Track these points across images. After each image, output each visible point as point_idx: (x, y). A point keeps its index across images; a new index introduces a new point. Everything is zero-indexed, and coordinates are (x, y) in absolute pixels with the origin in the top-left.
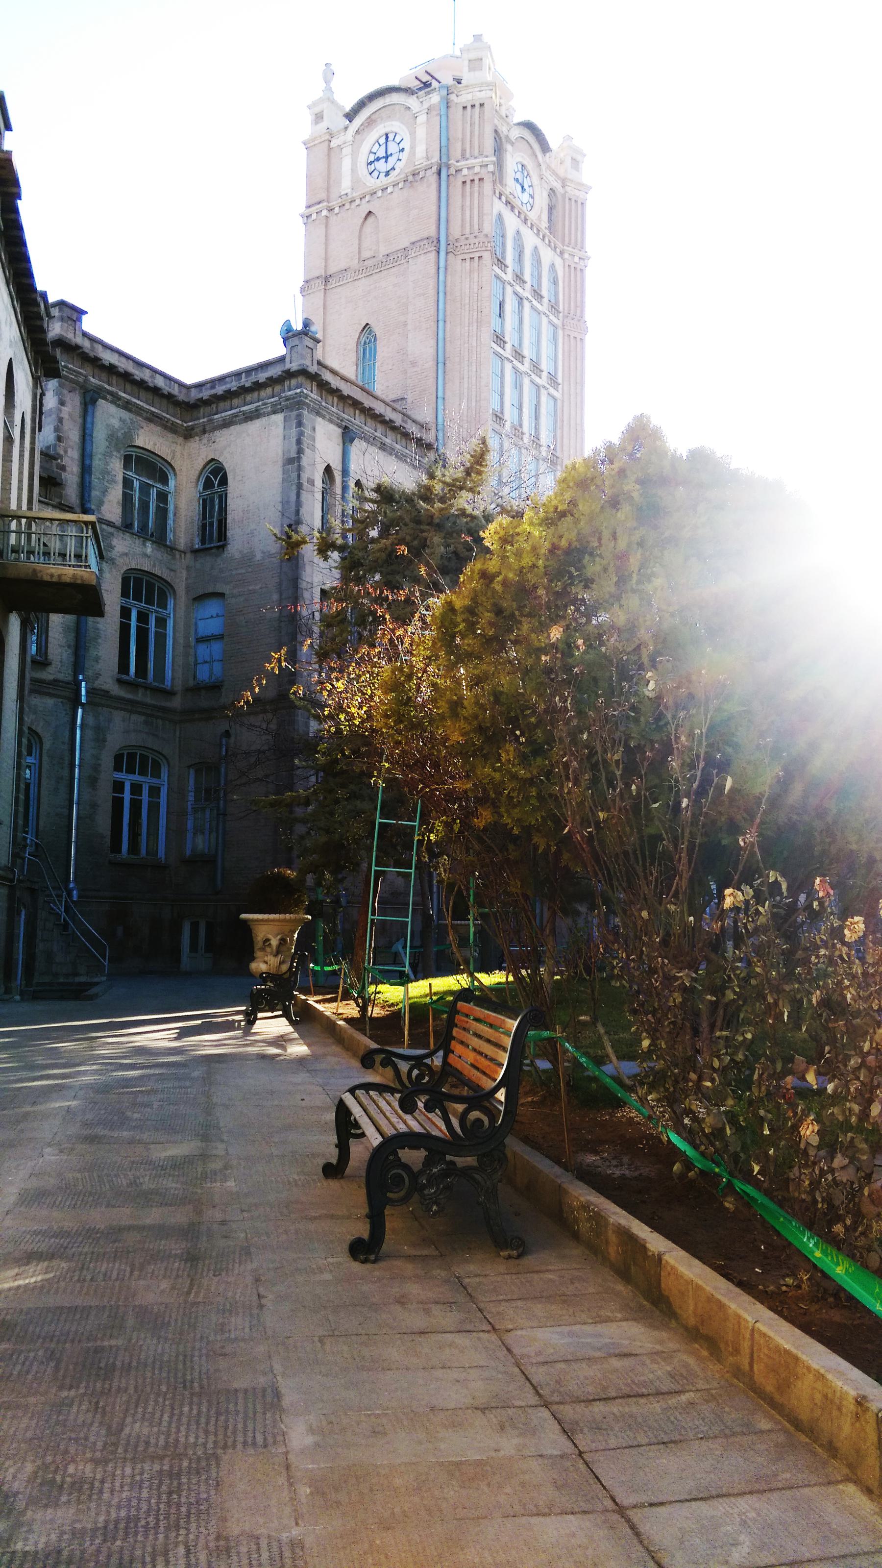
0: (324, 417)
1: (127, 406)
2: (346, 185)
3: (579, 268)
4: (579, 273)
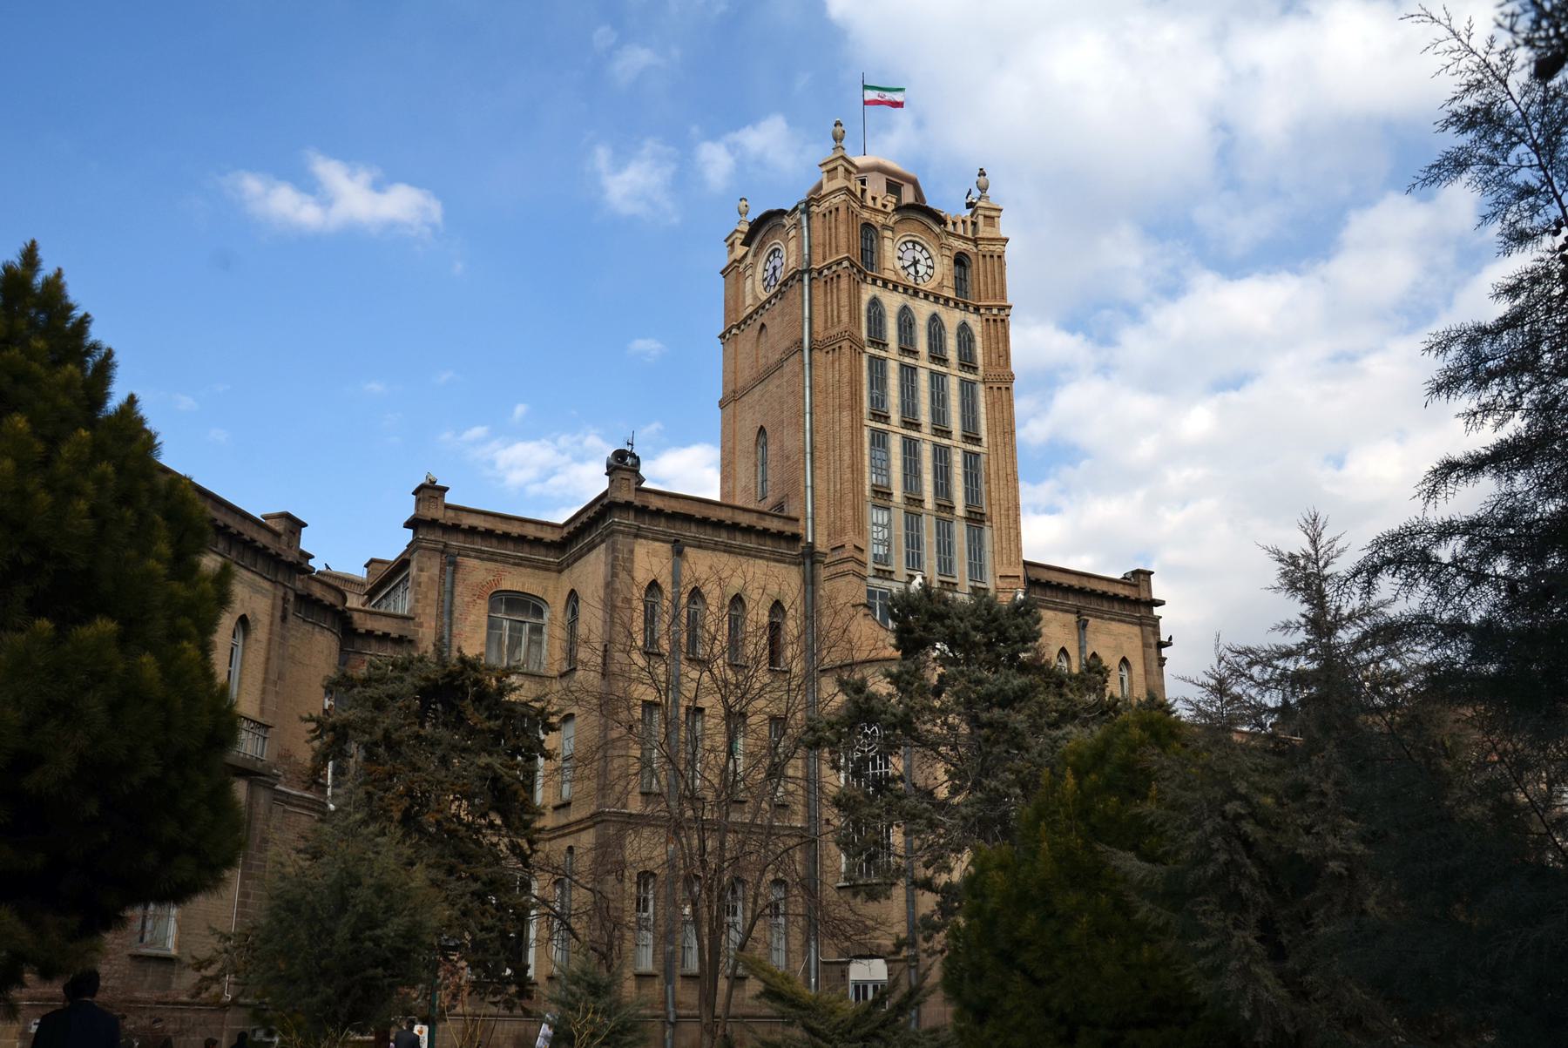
0: (646, 538)
1: (492, 557)
2: (749, 301)
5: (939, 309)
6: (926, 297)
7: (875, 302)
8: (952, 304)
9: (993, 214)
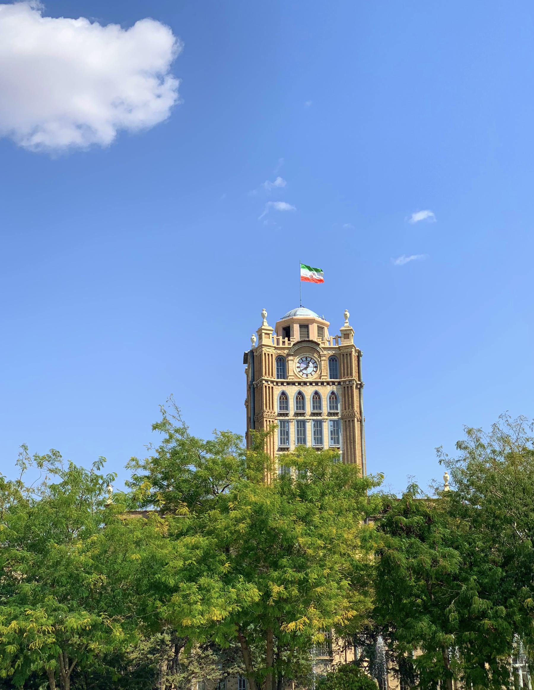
3: (349, 386)
4: (349, 388)
5: (316, 388)
6: (311, 384)
7: (283, 393)
8: (325, 384)
9: (348, 332)
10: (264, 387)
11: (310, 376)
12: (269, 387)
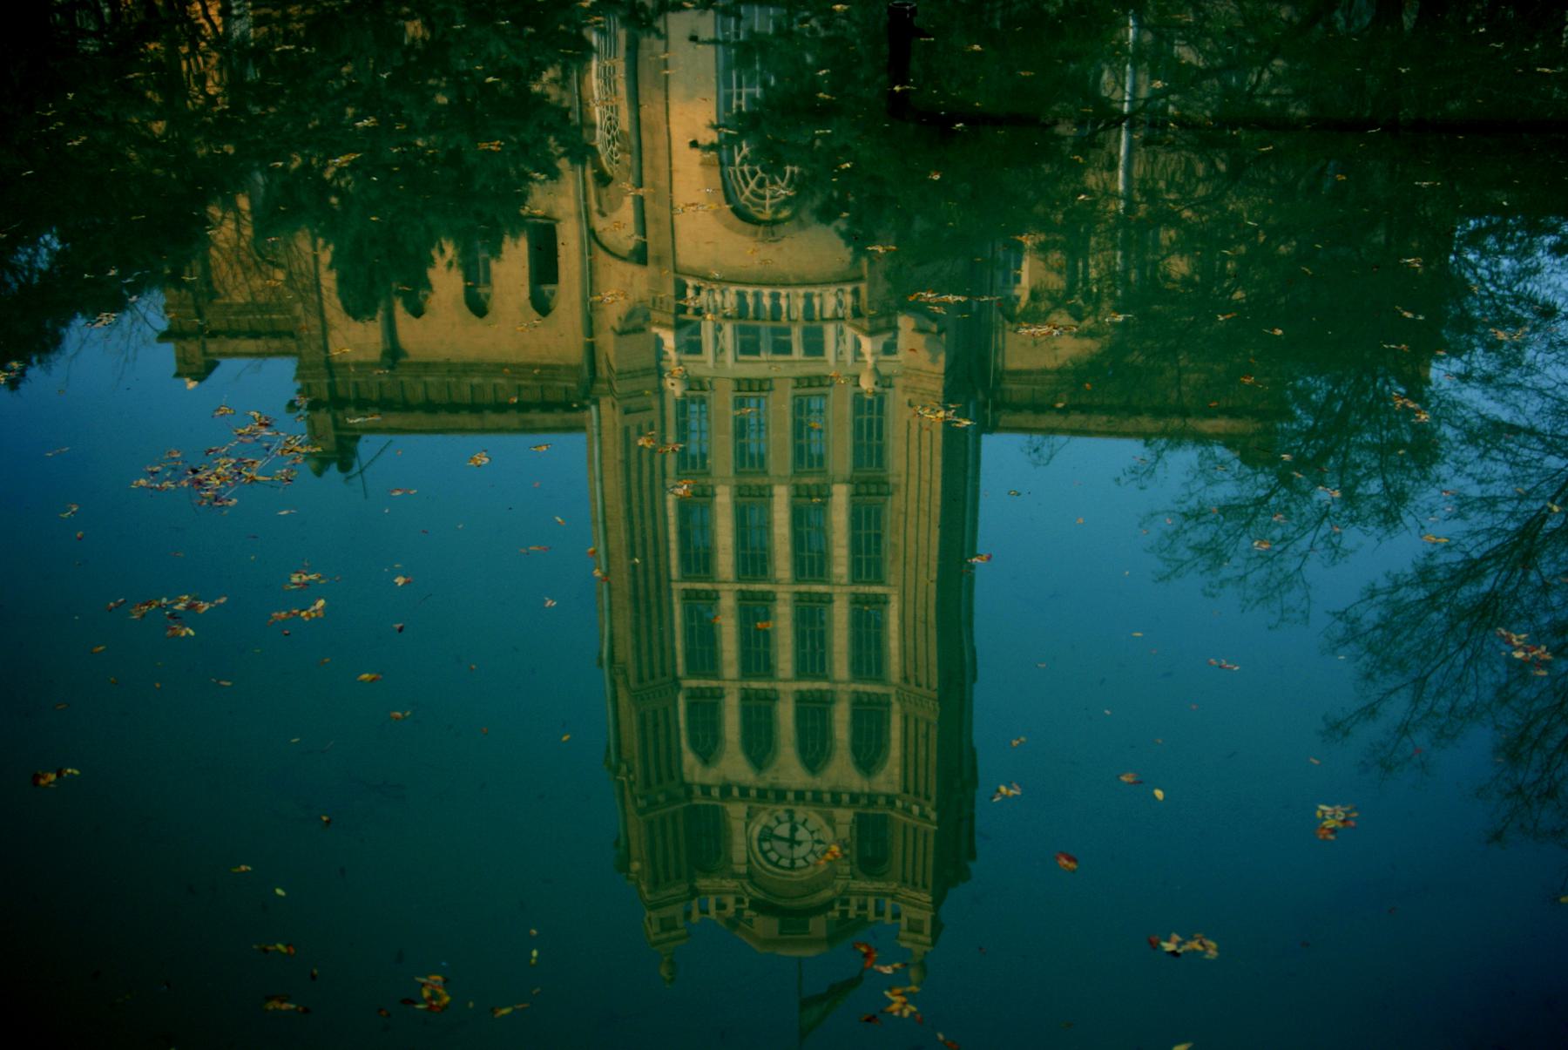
10: (934, 799)
11: (785, 817)
12: (917, 793)
